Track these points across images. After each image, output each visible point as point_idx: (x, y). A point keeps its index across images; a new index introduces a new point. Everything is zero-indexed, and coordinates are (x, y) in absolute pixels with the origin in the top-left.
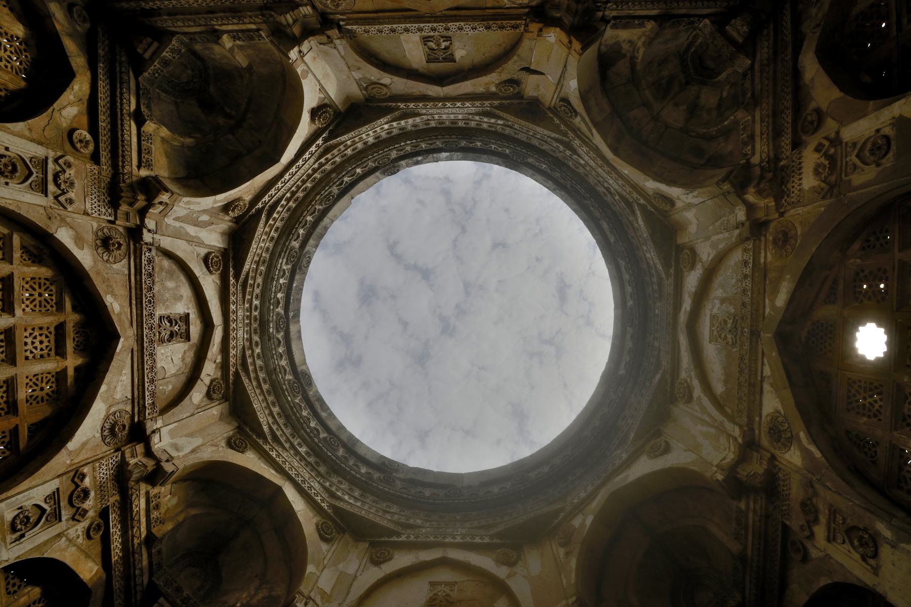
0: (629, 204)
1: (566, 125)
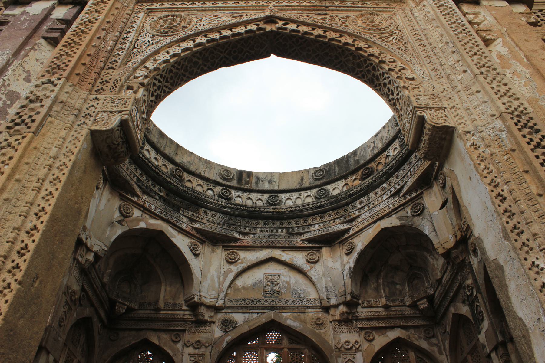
1: (409, 201)
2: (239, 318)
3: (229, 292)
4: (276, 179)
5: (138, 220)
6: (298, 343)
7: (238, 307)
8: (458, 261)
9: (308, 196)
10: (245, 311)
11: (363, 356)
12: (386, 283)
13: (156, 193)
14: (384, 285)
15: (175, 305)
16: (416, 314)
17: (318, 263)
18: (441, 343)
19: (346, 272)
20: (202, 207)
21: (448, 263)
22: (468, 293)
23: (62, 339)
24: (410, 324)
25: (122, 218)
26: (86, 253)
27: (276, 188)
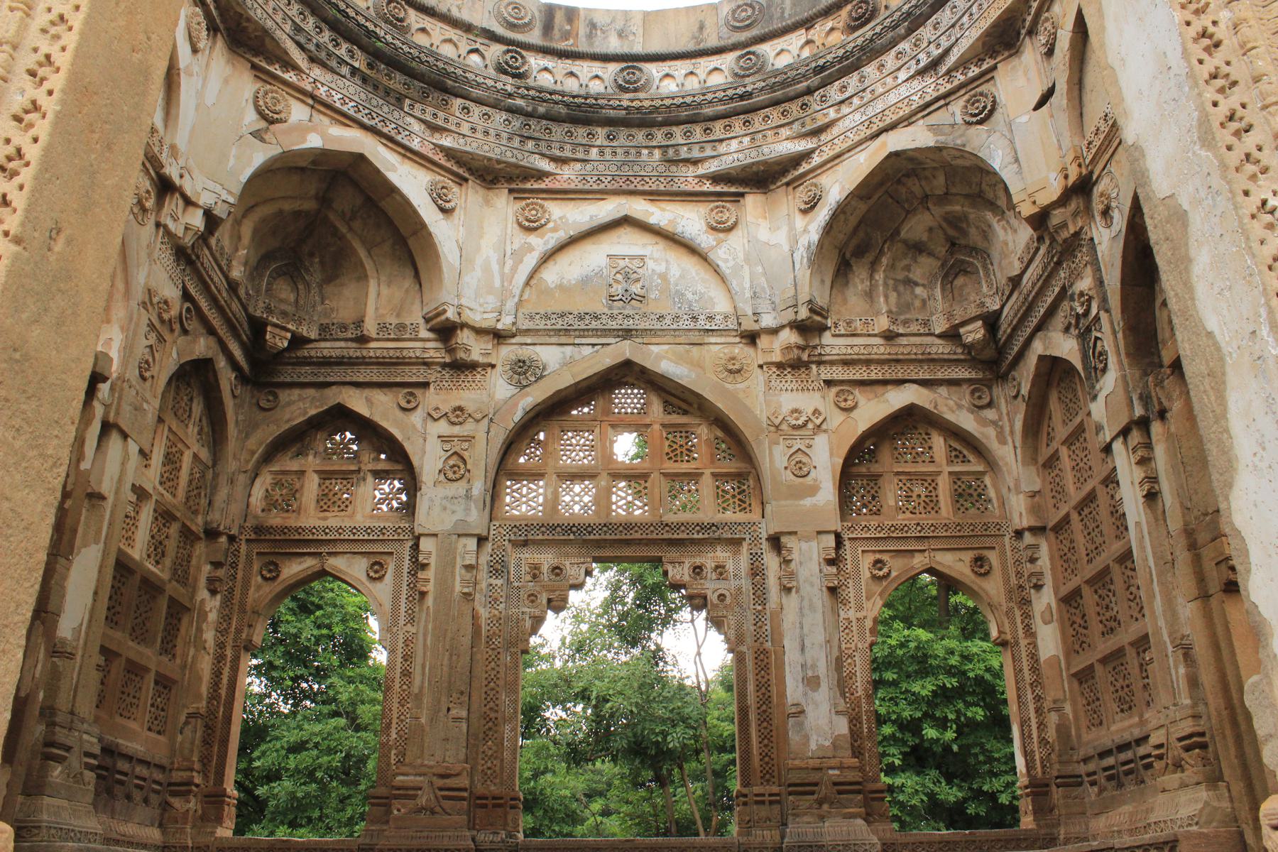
0: (817, 132)
2: (549, 355)
3: (526, 296)
4: (636, 26)
5: (302, 130)
6: (685, 413)
7: (547, 332)
8: (1065, 234)
9: (716, 69)
10: (564, 340)
11: (830, 443)
12: (891, 282)
13: (342, 62)
14: (885, 284)
15: (401, 327)
16: (955, 353)
17: (734, 232)
18: (1006, 418)
19: (801, 255)
20: (457, 96)
21: (1040, 239)
22: (1080, 310)
23: (152, 407)
24: (940, 376)
25: (263, 124)
26: (184, 211)
27: (638, 49)
